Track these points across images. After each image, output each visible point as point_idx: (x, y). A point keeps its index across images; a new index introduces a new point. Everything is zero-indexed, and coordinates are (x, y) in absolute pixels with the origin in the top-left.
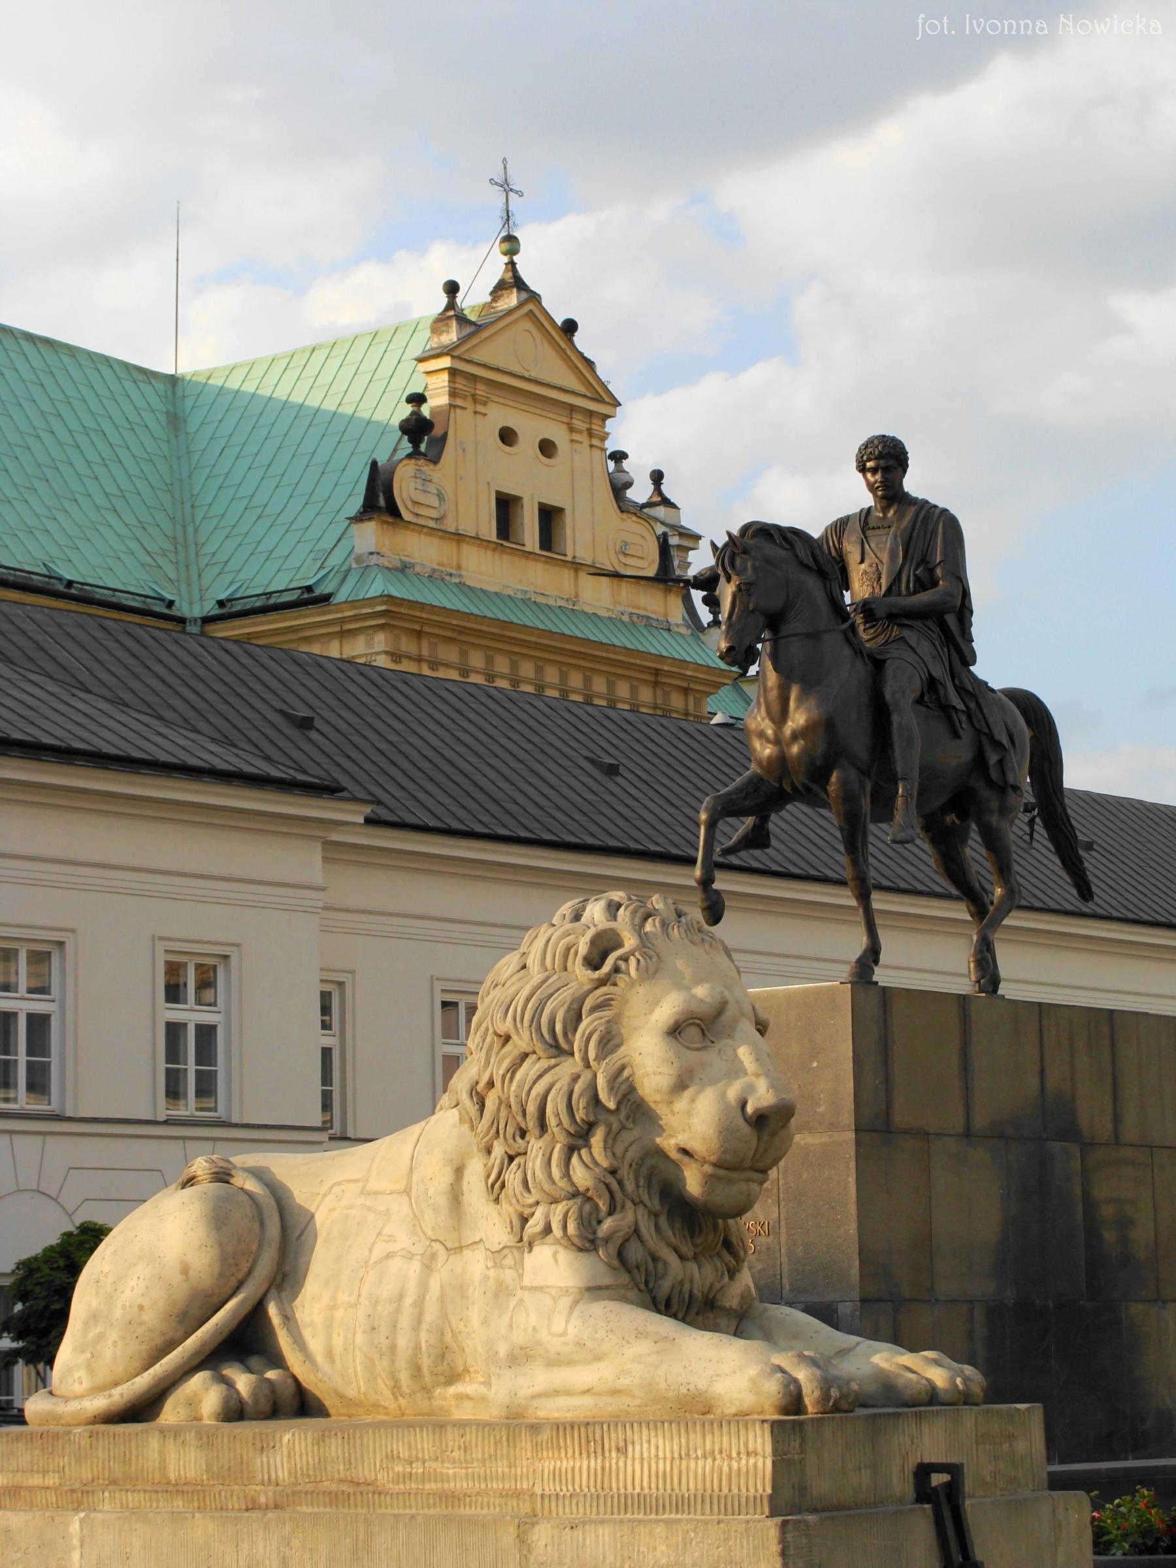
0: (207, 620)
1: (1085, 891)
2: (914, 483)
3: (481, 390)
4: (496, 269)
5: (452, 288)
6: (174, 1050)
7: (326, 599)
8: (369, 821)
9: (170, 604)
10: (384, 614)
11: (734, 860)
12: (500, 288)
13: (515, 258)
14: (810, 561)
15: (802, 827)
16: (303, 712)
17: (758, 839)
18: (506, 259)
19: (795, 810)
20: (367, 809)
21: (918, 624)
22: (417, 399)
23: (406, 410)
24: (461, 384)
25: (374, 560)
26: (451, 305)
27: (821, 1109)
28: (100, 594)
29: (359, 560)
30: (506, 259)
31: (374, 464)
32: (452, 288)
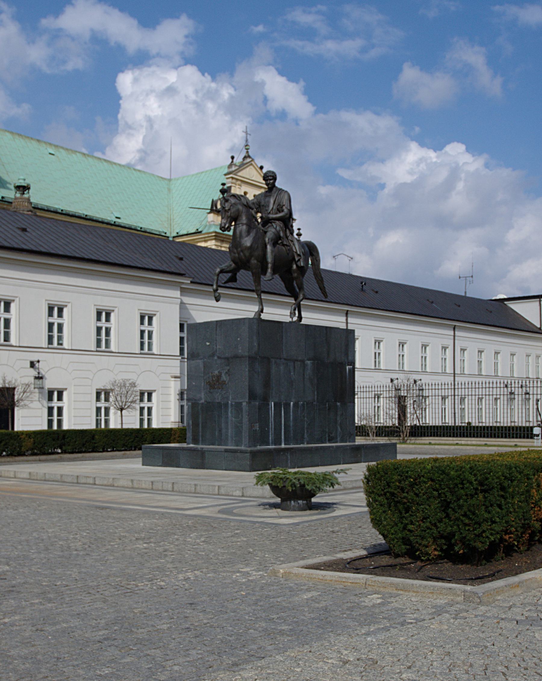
0: (174, 237)
1: (326, 295)
2: (278, 184)
3: (239, 182)
4: (244, 154)
5: (233, 158)
6: (142, 337)
7: (201, 232)
8: (192, 282)
9: (166, 233)
10: (215, 236)
11: (227, 285)
12: (245, 158)
13: (249, 150)
14: (245, 203)
15: (244, 276)
16: (181, 256)
17: (233, 279)
18: (246, 151)
19: (242, 271)
20: (191, 279)
21: (277, 222)
22: (223, 184)
23: (221, 187)
24: (234, 181)
25: (212, 223)
26: (232, 162)
27: (240, 351)
28: (148, 231)
29: (209, 222)
30: (246, 151)
31: (213, 201)
32: (233, 158)
